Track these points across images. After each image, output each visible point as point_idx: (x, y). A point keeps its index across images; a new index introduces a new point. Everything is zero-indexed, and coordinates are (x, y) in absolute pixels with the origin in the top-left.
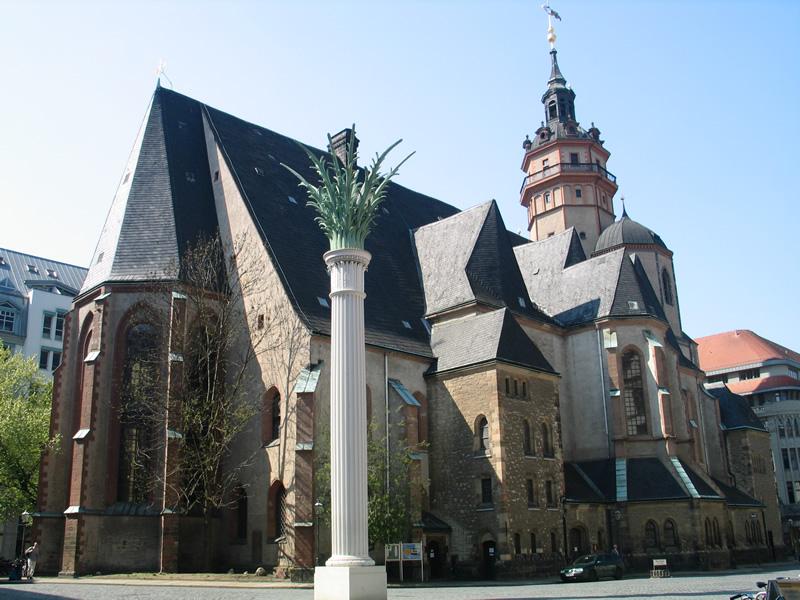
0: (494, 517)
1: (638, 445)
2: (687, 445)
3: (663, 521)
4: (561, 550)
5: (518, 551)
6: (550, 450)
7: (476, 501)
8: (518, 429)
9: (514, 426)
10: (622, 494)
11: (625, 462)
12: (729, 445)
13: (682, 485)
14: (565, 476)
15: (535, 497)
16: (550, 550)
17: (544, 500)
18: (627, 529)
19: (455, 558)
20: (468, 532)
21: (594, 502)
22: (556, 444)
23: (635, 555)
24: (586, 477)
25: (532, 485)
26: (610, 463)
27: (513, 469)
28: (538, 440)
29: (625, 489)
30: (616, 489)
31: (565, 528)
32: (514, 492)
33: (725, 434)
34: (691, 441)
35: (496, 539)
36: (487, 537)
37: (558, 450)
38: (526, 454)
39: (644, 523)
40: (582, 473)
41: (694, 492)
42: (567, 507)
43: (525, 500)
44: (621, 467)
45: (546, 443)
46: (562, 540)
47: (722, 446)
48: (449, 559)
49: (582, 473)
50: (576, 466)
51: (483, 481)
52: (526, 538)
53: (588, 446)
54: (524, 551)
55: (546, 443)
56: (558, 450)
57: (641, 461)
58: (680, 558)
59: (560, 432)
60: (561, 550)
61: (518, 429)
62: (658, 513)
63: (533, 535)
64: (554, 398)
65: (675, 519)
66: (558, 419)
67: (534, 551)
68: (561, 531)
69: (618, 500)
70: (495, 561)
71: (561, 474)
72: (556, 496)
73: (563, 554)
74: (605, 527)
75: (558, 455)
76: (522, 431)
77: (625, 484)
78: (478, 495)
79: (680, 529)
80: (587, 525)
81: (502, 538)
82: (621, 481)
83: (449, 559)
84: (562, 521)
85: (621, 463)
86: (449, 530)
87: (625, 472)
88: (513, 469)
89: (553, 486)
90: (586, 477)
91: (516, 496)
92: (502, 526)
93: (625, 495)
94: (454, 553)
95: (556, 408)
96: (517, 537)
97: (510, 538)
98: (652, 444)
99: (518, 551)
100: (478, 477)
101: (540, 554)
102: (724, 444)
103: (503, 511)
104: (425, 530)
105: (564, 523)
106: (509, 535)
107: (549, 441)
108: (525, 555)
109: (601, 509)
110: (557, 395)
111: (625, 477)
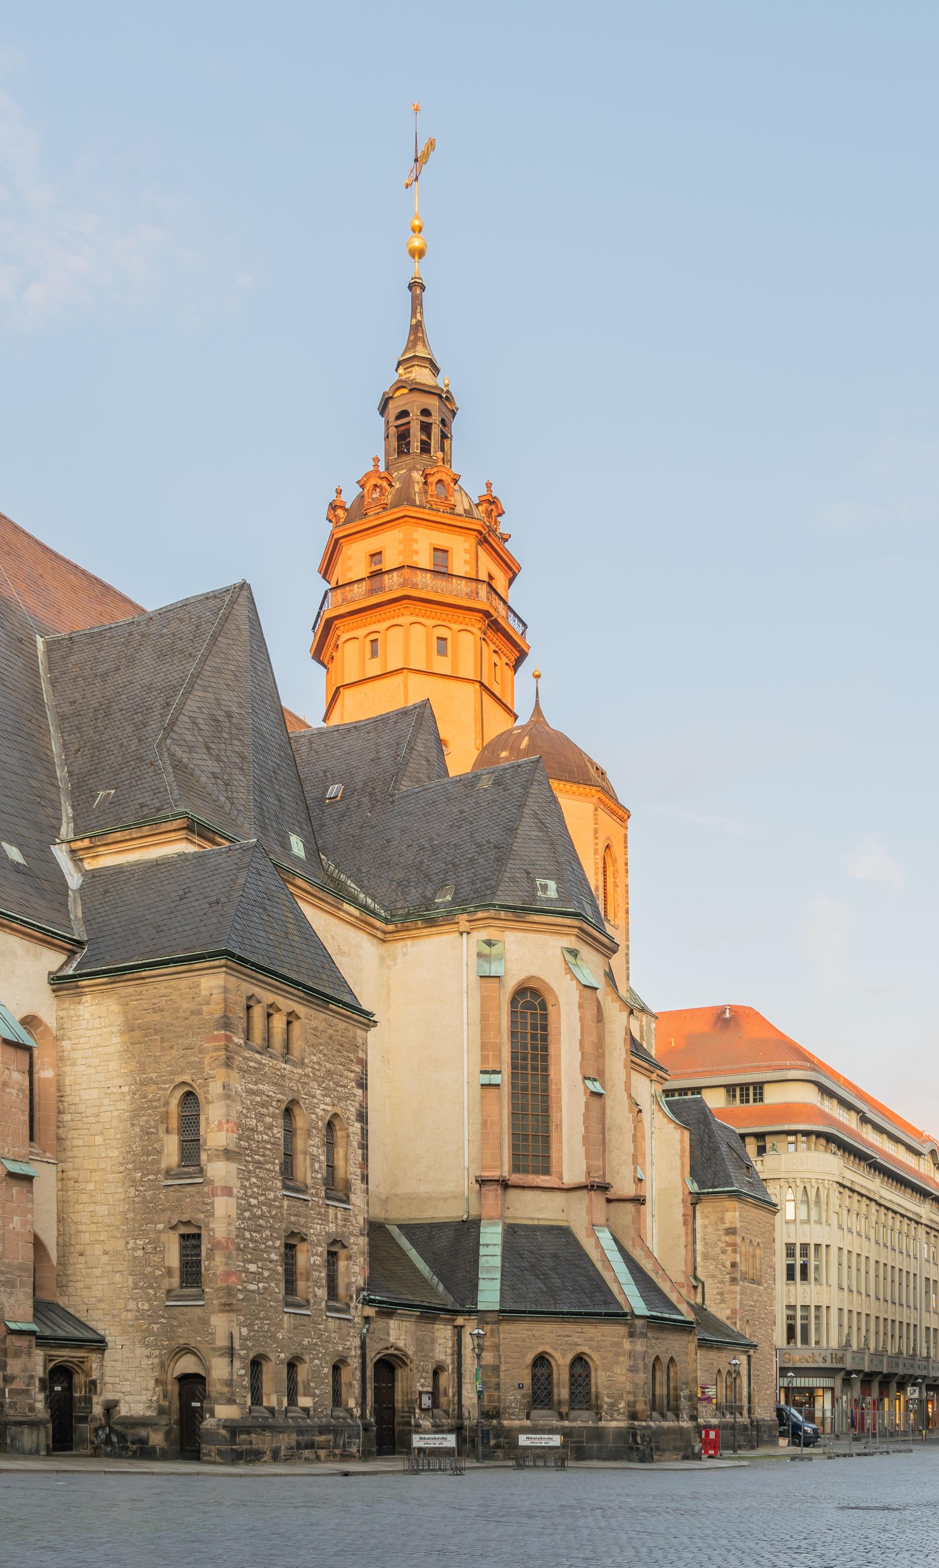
0: (205, 1322)
1: (529, 1196)
2: (630, 1207)
3: (570, 1356)
4: (352, 1403)
5: (257, 1399)
6: (340, 1185)
7: (166, 1283)
8: (270, 1127)
9: (260, 1117)
10: (489, 1294)
11: (499, 1229)
12: (699, 1222)
13: (614, 1288)
14: (370, 1244)
15: (301, 1285)
16: (329, 1402)
17: (322, 1293)
18: (496, 1369)
19: (110, 1407)
20: (147, 1352)
21: (430, 1313)
22: (354, 1172)
23: (506, 1423)
24: (413, 1254)
25: (294, 1257)
26: (468, 1229)
27: (254, 1217)
28: (314, 1159)
29: (497, 1285)
30: (477, 1285)
31: (363, 1356)
32: (252, 1268)
33: (695, 1200)
34: (639, 1201)
35: (208, 1369)
36: (187, 1365)
37: (358, 1185)
38: (286, 1187)
39: (530, 1358)
40: (404, 1243)
41: (639, 1306)
42: (370, 1311)
43: (279, 1289)
44: (491, 1238)
45: (331, 1167)
46: (357, 1385)
47: (685, 1223)
48: (98, 1410)
49: (404, 1243)
50: (395, 1232)
51: (183, 1237)
52: (273, 1375)
53: (424, 1189)
54: (273, 1399)
55: (331, 1167)
56: (358, 1185)
57: (533, 1230)
58: (598, 1434)
59: (364, 1147)
60: (352, 1403)
61: (270, 1127)
62: (560, 1341)
63: (292, 1366)
64: (358, 1069)
65: (594, 1355)
66: (362, 1117)
67: (292, 1401)
68: (355, 1363)
69: (481, 1307)
70: (203, 1418)
71: (363, 1241)
72: (348, 1286)
73: (357, 1412)
74: (449, 1360)
75: (357, 1199)
76: (278, 1132)
77: (498, 1276)
78: (169, 1271)
79: (600, 1379)
80: (410, 1353)
81: (219, 1370)
82: (489, 1269)
83: (98, 1410)
84: (358, 1342)
85: (490, 1229)
86: (99, 1344)
87: (498, 1251)
88: (254, 1217)
89: (342, 1264)
90: (413, 1254)
91: (257, 1277)
92: (221, 1342)
93: (497, 1297)
94: (109, 1396)
95: (359, 1092)
96: (256, 1364)
97: (241, 1370)
98: (559, 1199)
99: (257, 1399)
100: (173, 1228)
101: (306, 1410)
102: (690, 1220)
103: (228, 1308)
104: (42, 1341)
105: (363, 1346)
106: (237, 1364)
107: (340, 1163)
108: (271, 1410)
109: (443, 1333)
110: (363, 1063)
111: (497, 1262)
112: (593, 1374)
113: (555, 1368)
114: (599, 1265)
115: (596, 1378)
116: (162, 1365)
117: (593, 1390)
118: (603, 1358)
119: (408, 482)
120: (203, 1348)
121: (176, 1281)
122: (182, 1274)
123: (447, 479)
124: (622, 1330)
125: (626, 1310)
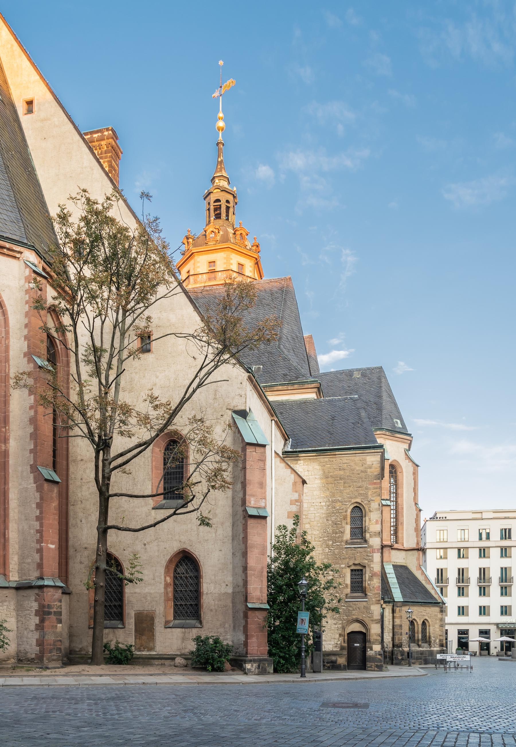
82: (394, 583)
112: (428, 628)
113: (416, 626)
114: (424, 582)
115: (429, 629)
116: (344, 628)
117: (428, 634)
118: (432, 621)
119: (227, 232)
120: (367, 620)
121: (348, 590)
122: (352, 587)
123: (244, 234)
124: (437, 609)
125: (439, 601)
